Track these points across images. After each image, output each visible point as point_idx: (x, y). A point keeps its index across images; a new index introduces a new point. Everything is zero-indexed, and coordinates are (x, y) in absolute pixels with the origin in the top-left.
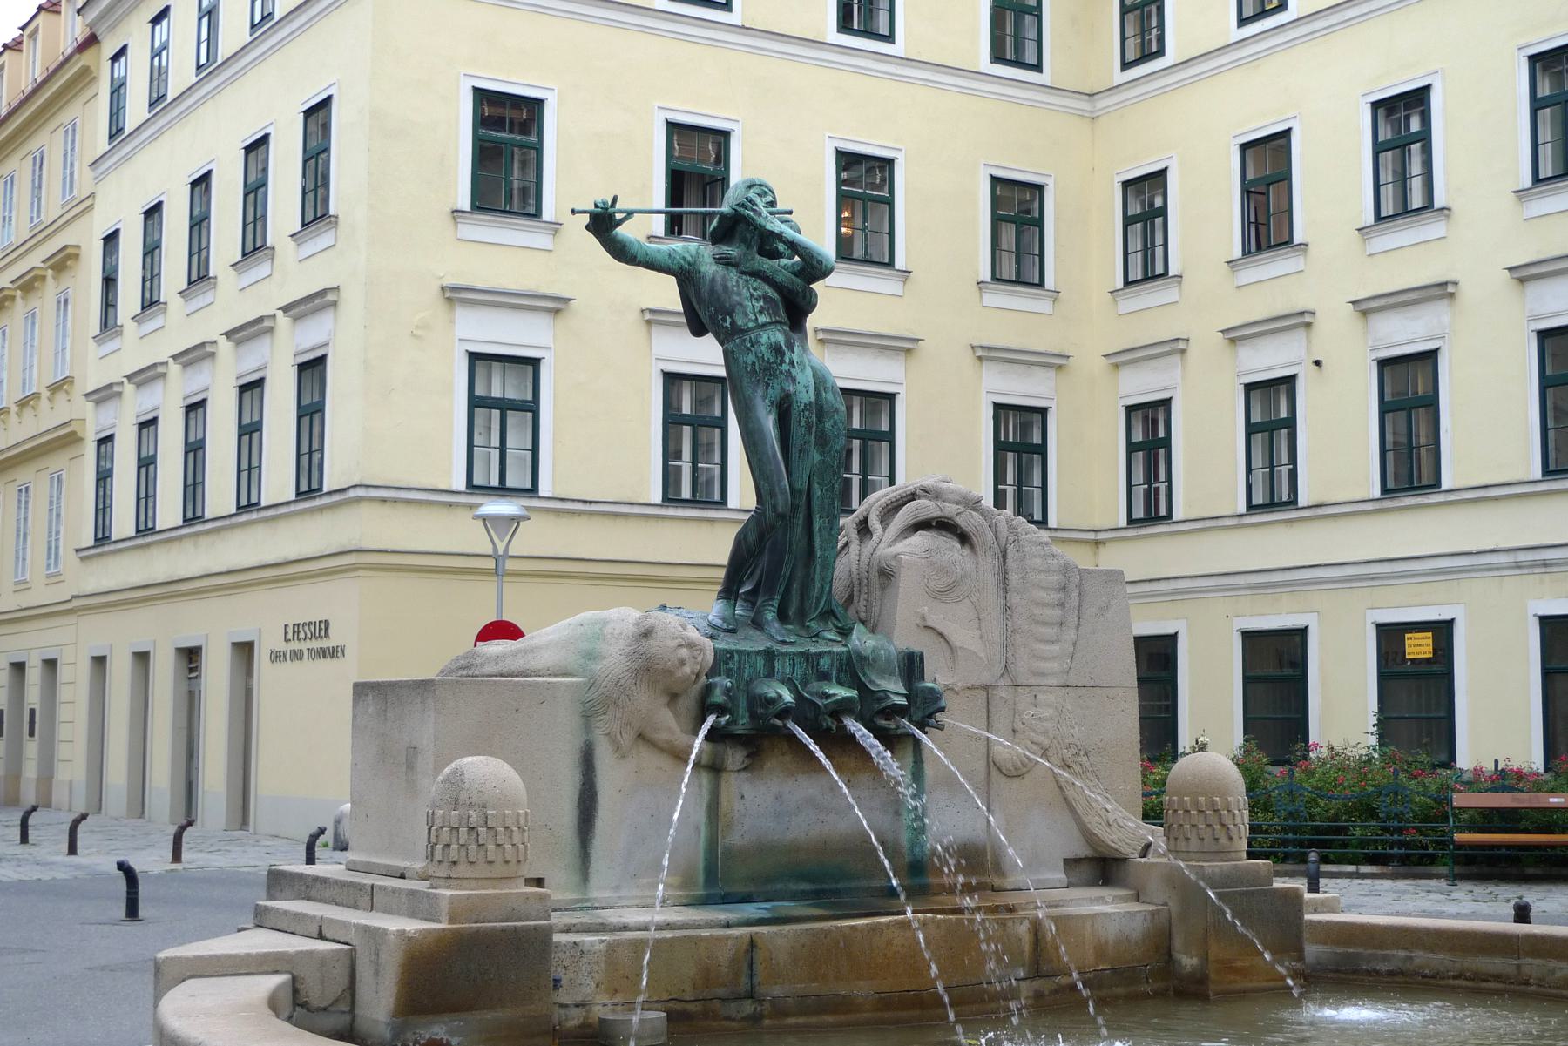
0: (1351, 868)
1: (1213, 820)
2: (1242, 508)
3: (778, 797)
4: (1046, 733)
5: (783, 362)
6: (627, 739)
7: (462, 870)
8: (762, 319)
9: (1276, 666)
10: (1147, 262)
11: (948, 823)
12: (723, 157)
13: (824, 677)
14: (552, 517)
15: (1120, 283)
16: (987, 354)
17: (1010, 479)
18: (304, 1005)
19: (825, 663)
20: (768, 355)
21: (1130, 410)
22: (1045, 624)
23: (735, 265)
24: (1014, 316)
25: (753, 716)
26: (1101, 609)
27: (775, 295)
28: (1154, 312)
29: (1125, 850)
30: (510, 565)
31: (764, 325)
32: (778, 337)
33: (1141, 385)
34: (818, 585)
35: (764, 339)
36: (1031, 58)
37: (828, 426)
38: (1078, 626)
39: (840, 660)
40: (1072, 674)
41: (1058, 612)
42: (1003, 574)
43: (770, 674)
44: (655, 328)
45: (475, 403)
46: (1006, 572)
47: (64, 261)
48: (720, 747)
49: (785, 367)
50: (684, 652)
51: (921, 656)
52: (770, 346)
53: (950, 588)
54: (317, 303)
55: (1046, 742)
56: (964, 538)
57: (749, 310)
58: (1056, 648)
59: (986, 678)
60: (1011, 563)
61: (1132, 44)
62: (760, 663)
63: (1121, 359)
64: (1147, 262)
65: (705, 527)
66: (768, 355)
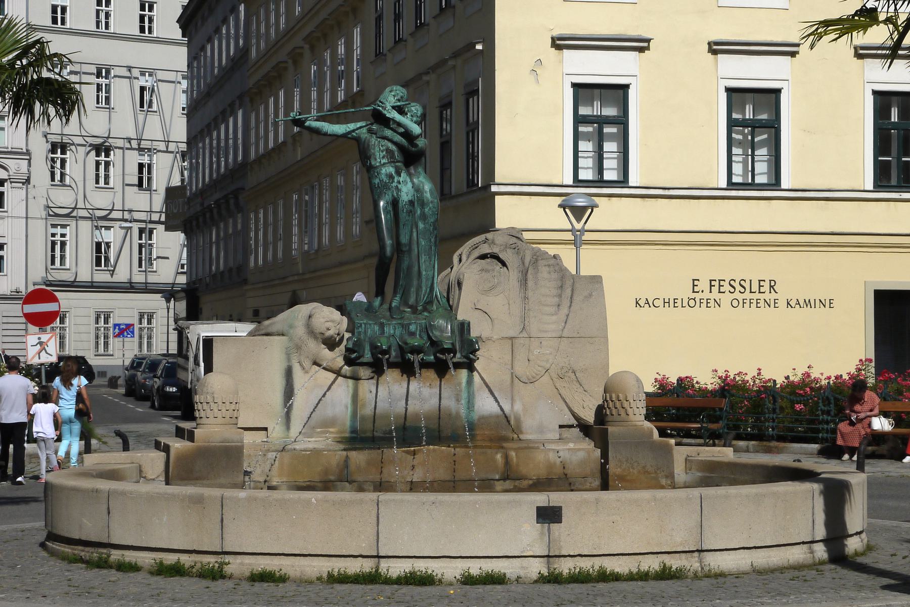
1: (618, 404)
4: (548, 361)
5: (393, 182)
6: (307, 364)
8: (384, 161)
11: (485, 405)
18: (145, 477)
19: (412, 328)
20: (385, 179)
22: (548, 305)
23: (375, 134)
25: (372, 354)
26: (586, 297)
27: (394, 148)
31: (384, 164)
32: (391, 170)
34: (424, 289)
35: (383, 171)
37: (426, 210)
38: (570, 306)
39: (421, 326)
40: (566, 330)
41: (556, 300)
45: (579, 120)
46: (526, 280)
48: (357, 368)
49: (394, 184)
50: (329, 325)
51: (469, 324)
52: (386, 175)
55: (548, 366)
56: (504, 264)
57: (378, 157)
58: (554, 318)
59: (511, 333)
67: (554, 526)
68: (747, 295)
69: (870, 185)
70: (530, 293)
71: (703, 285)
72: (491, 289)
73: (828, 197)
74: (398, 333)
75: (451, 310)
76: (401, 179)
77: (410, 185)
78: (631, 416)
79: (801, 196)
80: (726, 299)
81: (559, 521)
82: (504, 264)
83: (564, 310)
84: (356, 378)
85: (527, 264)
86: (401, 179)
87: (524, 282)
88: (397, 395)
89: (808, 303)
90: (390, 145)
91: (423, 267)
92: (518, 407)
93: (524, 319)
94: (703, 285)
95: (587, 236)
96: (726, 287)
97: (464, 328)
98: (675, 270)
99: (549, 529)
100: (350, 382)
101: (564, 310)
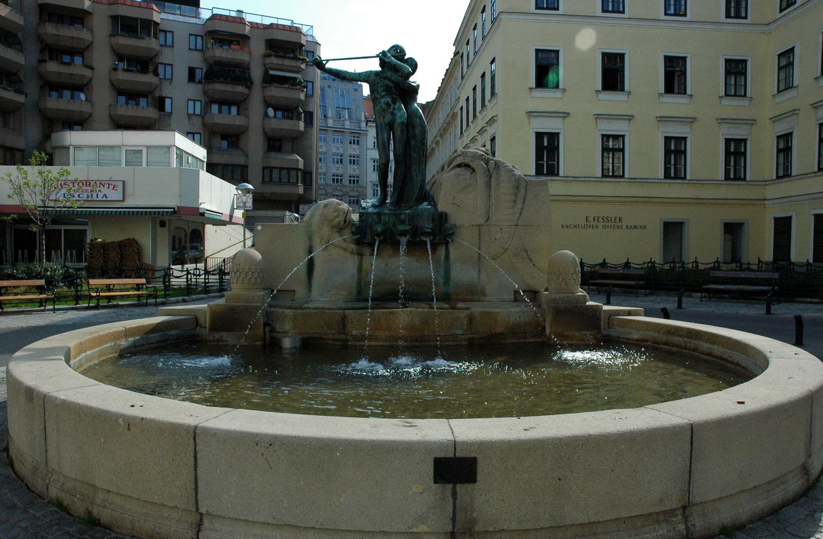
0: (809, 300)
2: (816, 170)
3: (387, 265)
9: (783, 226)
10: (786, 84)
12: (623, 61)
13: (403, 222)
15: (776, 92)
17: (732, 164)
21: (778, 137)
24: (734, 107)
28: (789, 100)
29: (538, 289)
33: (782, 128)
36: (743, 15)
41: (513, 197)
42: (488, 186)
43: (379, 222)
47: (454, 116)
50: (336, 214)
54: (492, 121)
60: (493, 179)
62: (375, 217)
63: (775, 119)
64: (786, 84)
66: (384, 107)
68: (610, 224)
70: (493, 193)
72: (464, 189)
73: (644, 181)
74: (391, 221)
76: (396, 107)
79: (633, 180)
81: (473, 480)
82: (474, 170)
83: (519, 205)
84: (361, 255)
85: (491, 170)
86: (396, 107)
87: (488, 186)
88: (402, 267)
89: (635, 227)
90: (389, 83)
93: (488, 212)
94: (591, 219)
96: (601, 220)
97: (442, 218)
99: (454, 494)
100: (356, 258)
101: (519, 205)
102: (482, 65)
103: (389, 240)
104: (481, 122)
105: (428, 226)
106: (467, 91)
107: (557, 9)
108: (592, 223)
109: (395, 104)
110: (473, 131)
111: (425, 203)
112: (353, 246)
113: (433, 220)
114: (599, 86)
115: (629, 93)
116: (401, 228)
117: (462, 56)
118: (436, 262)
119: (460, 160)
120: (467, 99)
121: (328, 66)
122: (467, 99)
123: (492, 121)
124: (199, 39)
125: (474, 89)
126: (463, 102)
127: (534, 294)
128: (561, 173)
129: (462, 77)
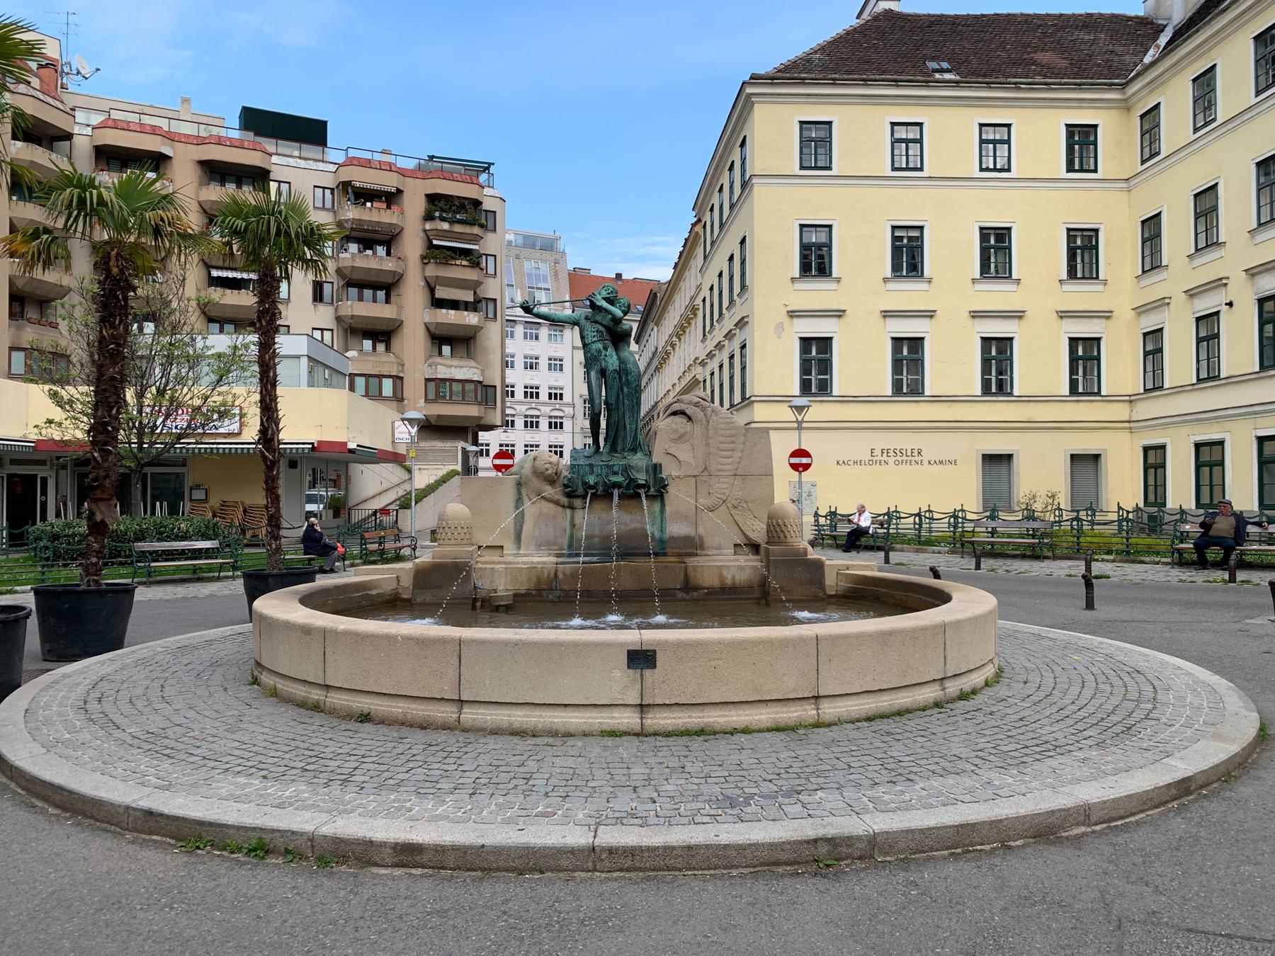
2: (1194, 381)
7: (452, 542)
10: (1152, 260)
13: (616, 473)
14: (838, 405)
16: (1063, 315)
17: (1081, 372)
28: (1158, 286)
30: (804, 425)
33: (1150, 323)
43: (592, 473)
44: (888, 320)
47: (694, 310)
53: (680, 438)
54: (742, 323)
56: (689, 418)
61: (1147, 150)
63: (1141, 310)
64: (1152, 260)
65: (914, 405)
67: (648, 673)
68: (904, 458)
69: (979, 393)
71: (877, 452)
75: (649, 454)
77: (615, 357)
78: (789, 539)
79: (937, 399)
80: (891, 460)
82: (689, 418)
84: (572, 507)
88: (616, 520)
89: (941, 462)
91: (627, 421)
92: (701, 530)
94: (877, 452)
95: (804, 425)
96: (892, 453)
97: (656, 468)
98: (860, 445)
100: (568, 511)
102: (730, 245)
103: (602, 494)
104: (728, 323)
105: (641, 478)
106: (711, 278)
107: (829, 168)
108: (879, 458)
109: (606, 349)
110: (718, 335)
111: (639, 455)
112: (565, 500)
113: (647, 471)
114: (888, 273)
115: (930, 281)
116: (614, 479)
117: (704, 226)
118: (651, 514)
119: (676, 407)
120: (712, 288)
121: (535, 310)
122: (712, 288)
123: (742, 323)
124: (328, 192)
125: (720, 275)
126: (705, 292)
127: (755, 547)
128: (836, 391)
129: (705, 257)
